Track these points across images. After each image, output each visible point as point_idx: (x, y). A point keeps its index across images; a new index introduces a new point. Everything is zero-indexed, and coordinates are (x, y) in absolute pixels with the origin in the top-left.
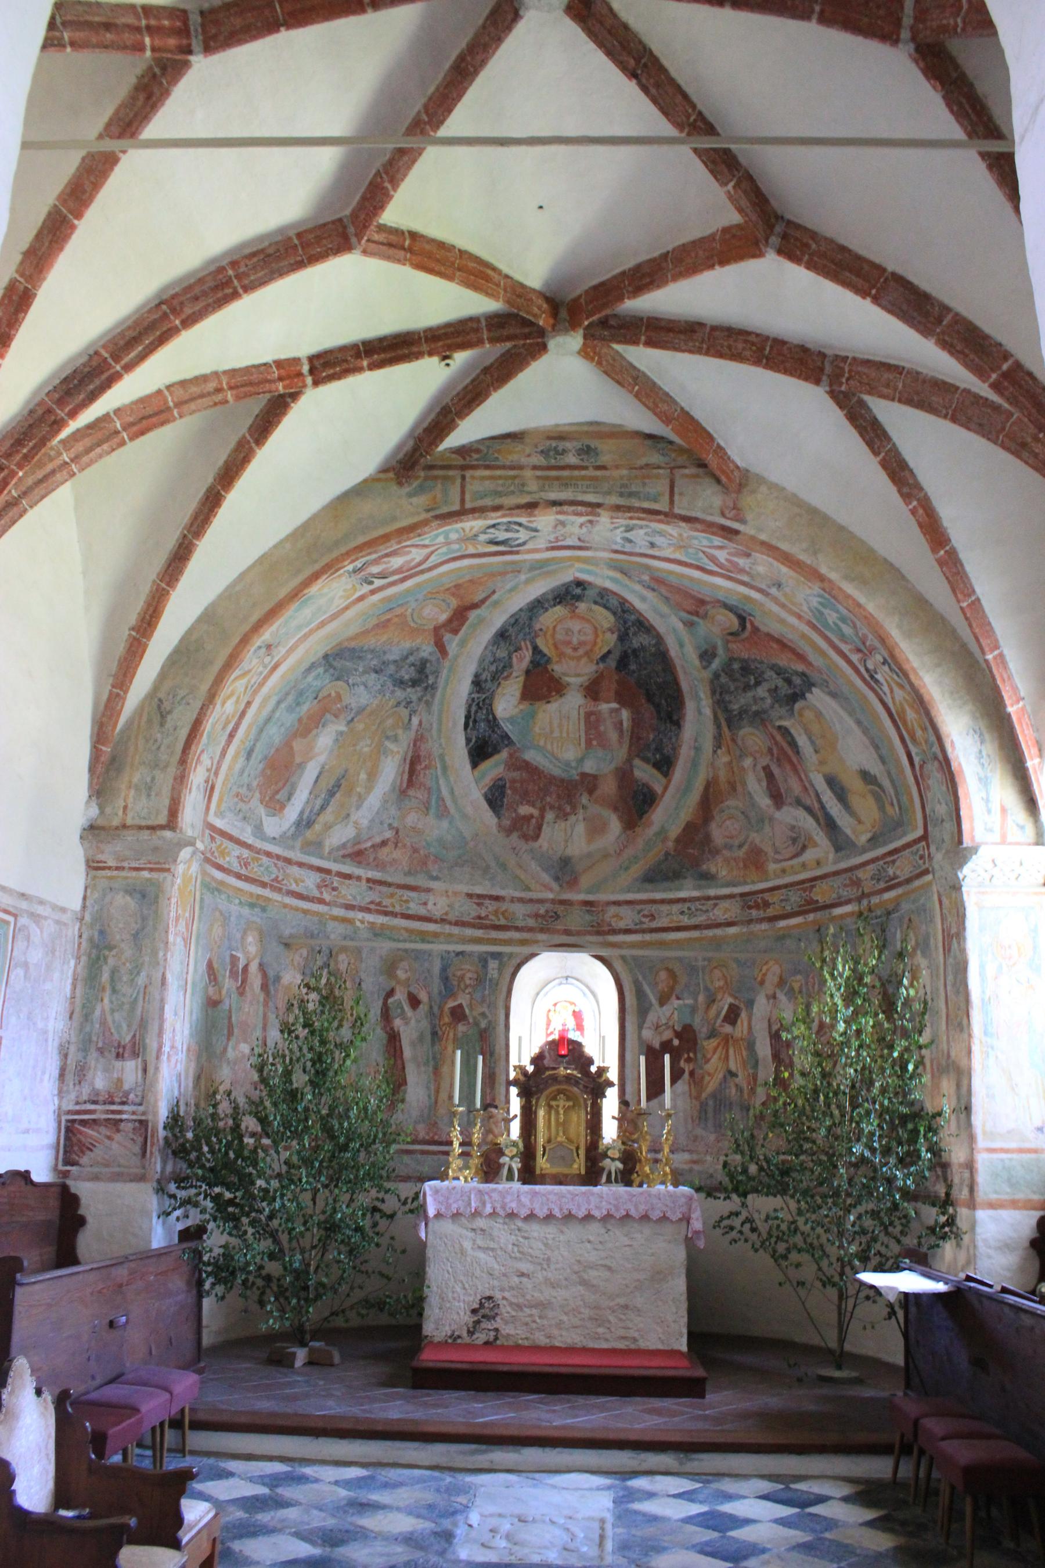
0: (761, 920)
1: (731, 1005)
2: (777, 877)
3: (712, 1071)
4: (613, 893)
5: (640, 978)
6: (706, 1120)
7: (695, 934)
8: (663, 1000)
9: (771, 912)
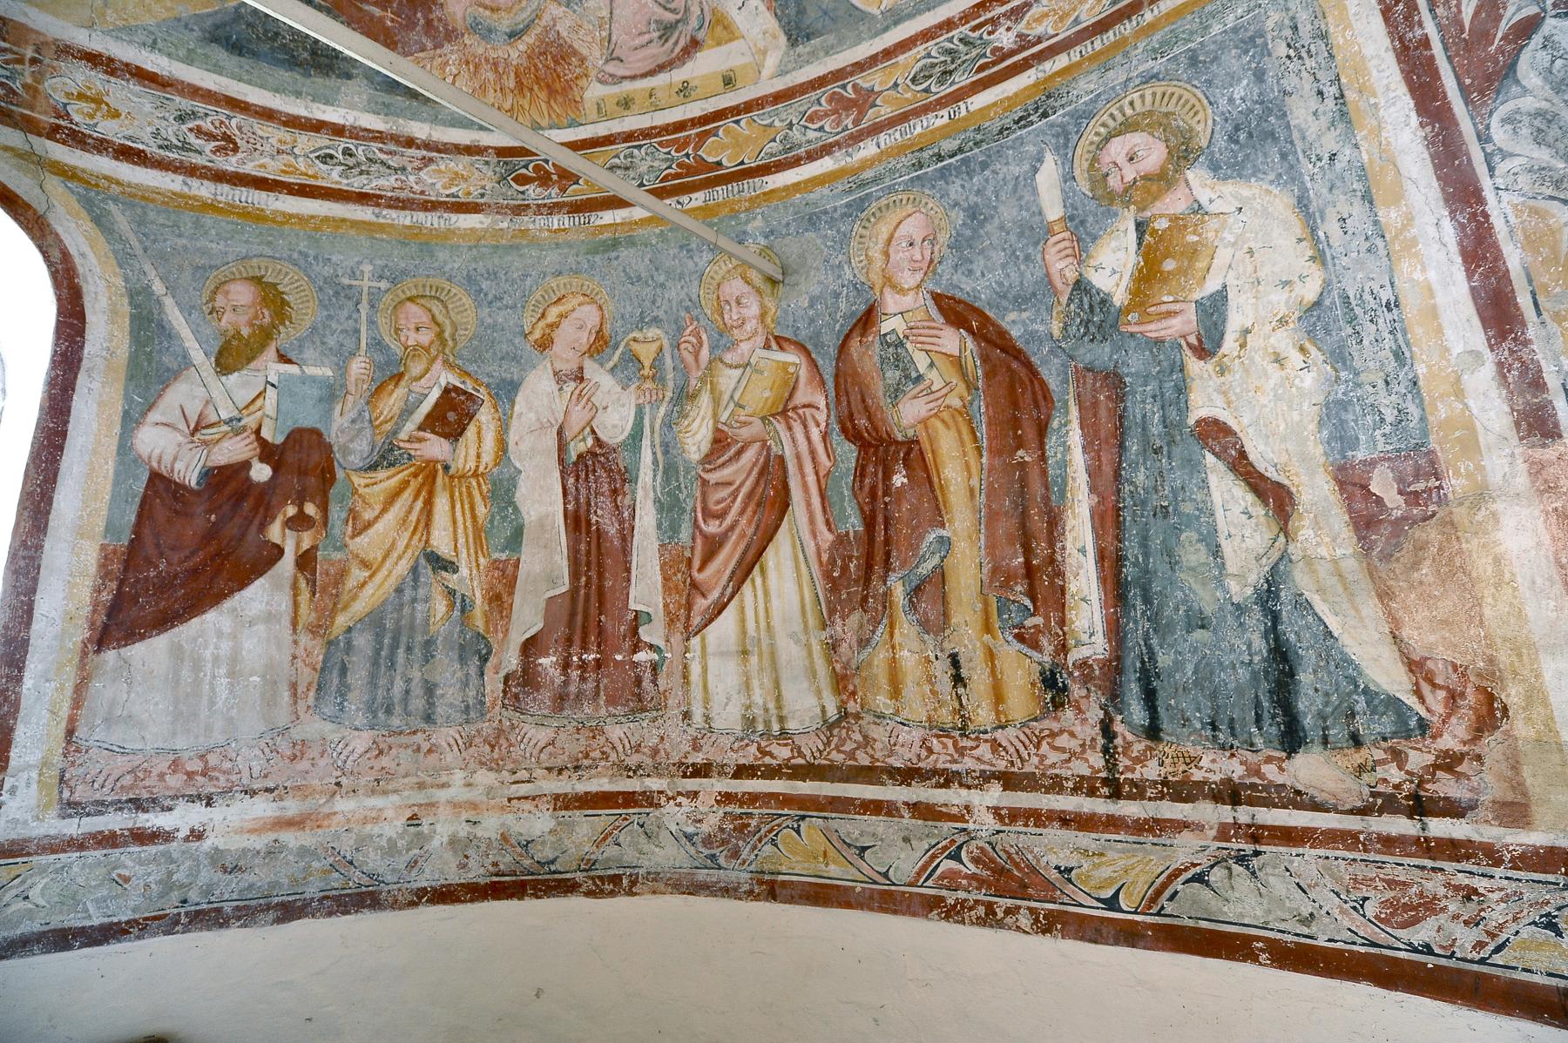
0: (554, 208)
1: (447, 391)
2: (602, 112)
3: (376, 555)
4: (91, 26)
5: (158, 287)
6: (343, 691)
7: (364, 213)
8: (229, 357)
9: (575, 193)
